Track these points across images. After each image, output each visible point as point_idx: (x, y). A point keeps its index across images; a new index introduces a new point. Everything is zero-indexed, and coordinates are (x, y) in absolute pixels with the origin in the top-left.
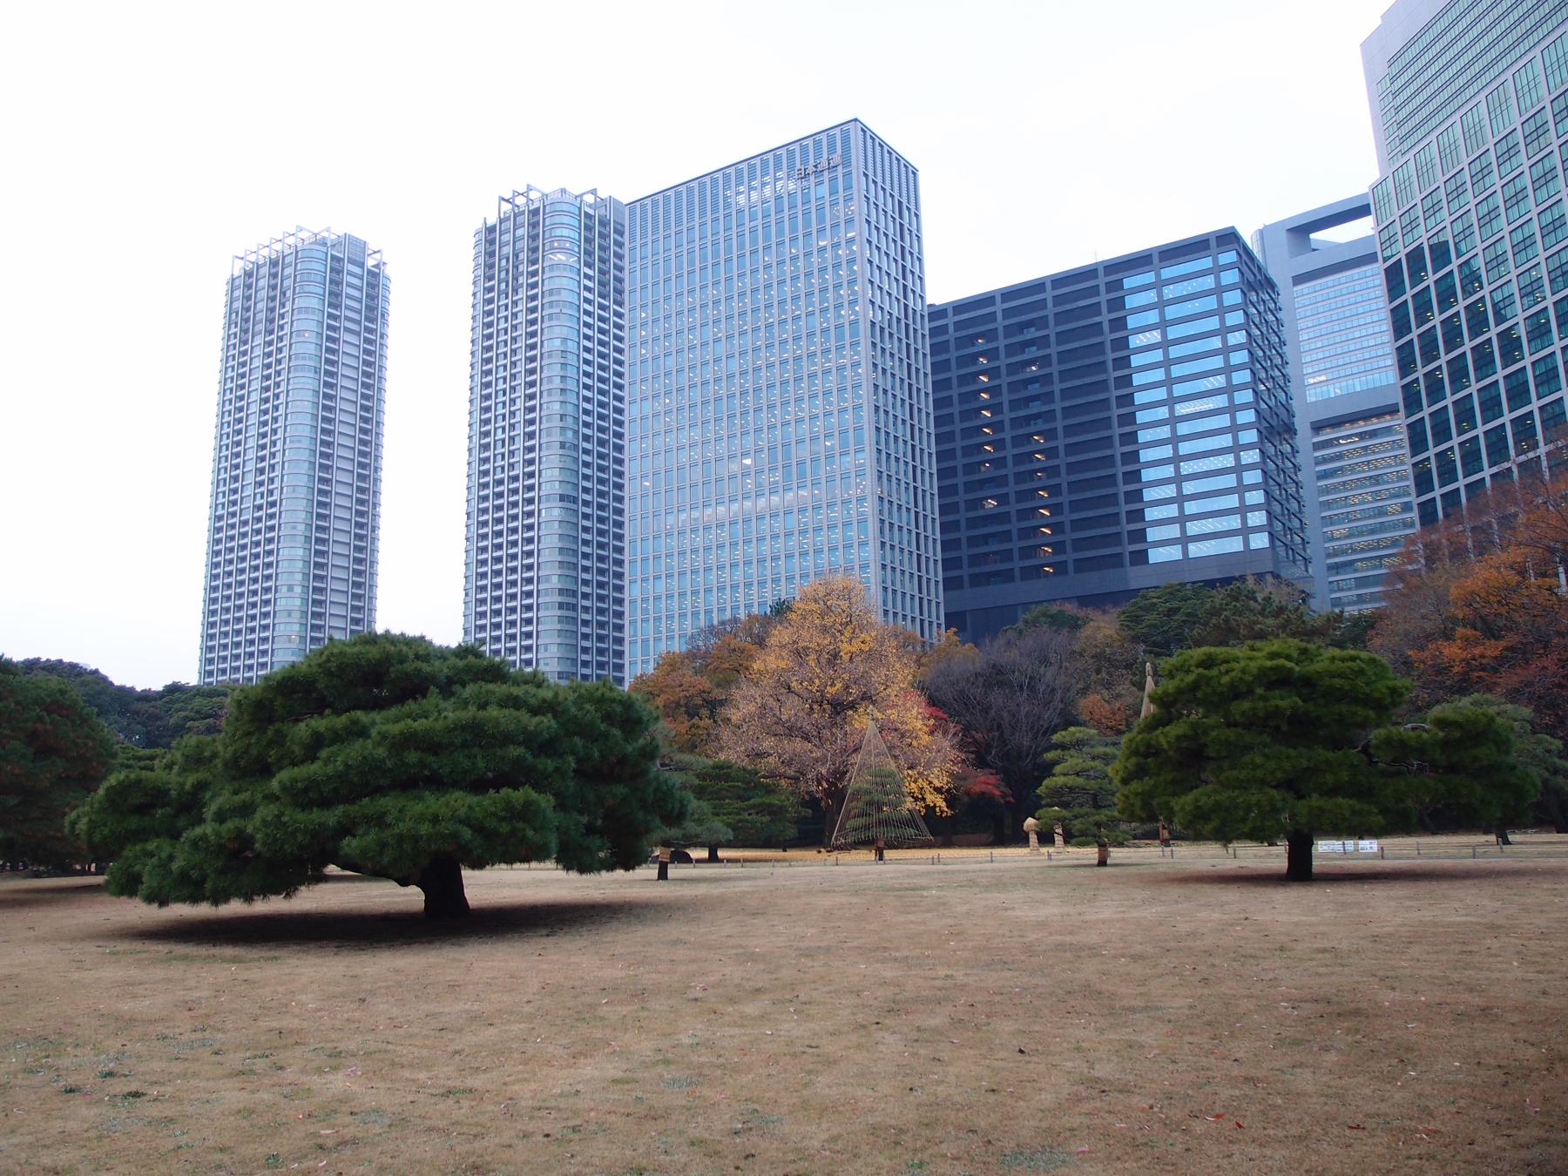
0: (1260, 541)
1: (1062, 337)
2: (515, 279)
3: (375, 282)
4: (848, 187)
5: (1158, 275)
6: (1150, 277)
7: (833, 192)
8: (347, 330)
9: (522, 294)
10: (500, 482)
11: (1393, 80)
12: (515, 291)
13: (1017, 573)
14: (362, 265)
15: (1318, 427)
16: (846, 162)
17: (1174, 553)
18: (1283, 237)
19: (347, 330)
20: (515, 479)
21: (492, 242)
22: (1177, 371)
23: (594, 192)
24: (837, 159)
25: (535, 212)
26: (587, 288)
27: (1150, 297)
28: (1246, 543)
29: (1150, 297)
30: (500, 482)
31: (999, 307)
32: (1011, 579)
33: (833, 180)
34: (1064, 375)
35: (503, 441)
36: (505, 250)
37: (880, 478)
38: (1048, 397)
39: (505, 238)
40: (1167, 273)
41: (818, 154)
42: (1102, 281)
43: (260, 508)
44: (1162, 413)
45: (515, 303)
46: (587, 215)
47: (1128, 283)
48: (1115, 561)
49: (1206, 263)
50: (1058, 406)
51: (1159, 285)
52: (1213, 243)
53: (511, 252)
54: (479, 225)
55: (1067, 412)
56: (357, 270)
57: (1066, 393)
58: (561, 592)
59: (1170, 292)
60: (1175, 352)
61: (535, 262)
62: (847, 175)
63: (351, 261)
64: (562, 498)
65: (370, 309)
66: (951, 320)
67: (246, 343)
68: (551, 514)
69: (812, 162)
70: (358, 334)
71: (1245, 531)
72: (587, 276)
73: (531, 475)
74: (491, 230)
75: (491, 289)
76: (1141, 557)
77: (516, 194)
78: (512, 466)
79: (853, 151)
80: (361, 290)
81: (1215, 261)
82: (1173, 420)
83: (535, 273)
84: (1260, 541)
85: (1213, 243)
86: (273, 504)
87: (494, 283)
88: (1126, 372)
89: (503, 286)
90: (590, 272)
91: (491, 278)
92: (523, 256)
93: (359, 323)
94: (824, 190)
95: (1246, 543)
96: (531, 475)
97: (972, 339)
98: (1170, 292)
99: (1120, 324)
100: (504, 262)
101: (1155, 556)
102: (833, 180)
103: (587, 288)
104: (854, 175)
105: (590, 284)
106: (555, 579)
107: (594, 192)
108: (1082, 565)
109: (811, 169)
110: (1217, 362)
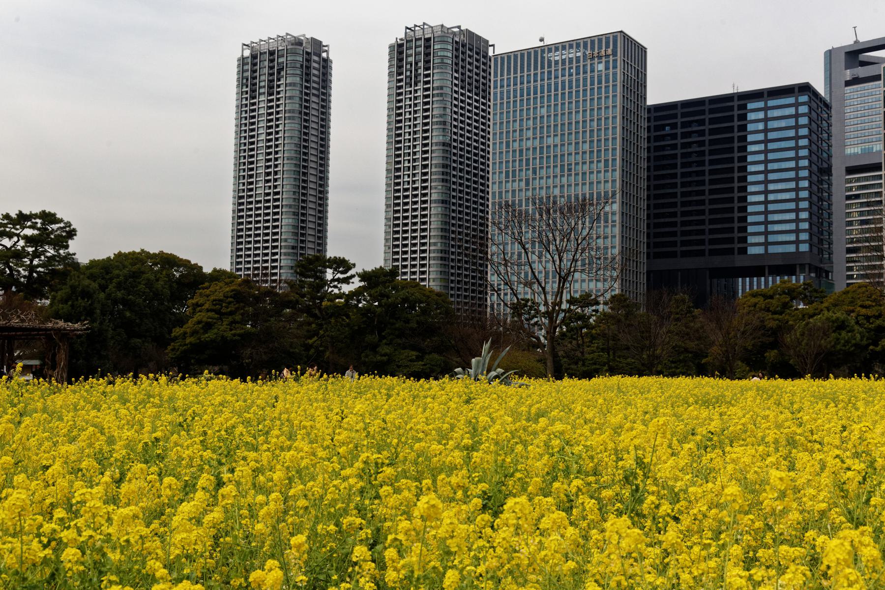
0: (804, 248)
1: (712, 132)
3: (326, 64)
5: (766, 104)
6: (761, 104)
8: (314, 95)
9: (420, 86)
10: (406, 190)
12: (416, 85)
13: (679, 253)
14: (319, 56)
15: (850, 170)
16: (614, 53)
17: (760, 250)
18: (843, 56)
19: (314, 95)
20: (416, 189)
21: (400, 53)
23: (459, 27)
24: (610, 51)
26: (456, 85)
28: (797, 248)
30: (406, 190)
31: (679, 111)
32: (676, 256)
33: (607, 62)
34: (712, 152)
35: (409, 167)
36: (410, 59)
39: (409, 52)
40: (771, 103)
42: (736, 103)
43: (268, 194)
45: (416, 91)
46: (456, 42)
47: (750, 106)
48: (731, 251)
49: (791, 100)
51: (766, 109)
52: (796, 90)
54: (393, 41)
55: (712, 172)
56: (316, 58)
57: (712, 162)
60: (771, 146)
61: (429, 69)
62: (615, 61)
63: (315, 54)
64: (443, 202)
65: (323, 81)
66: (653, 114)
67: (254, 98)
68: (435, 211)
70: (318, 96)
71: (797, 242)
72: (456, 78)
74: (400, 46)
76: (744, 251)
77: (416, 26)
83: (428, 76)
84: (804, 248)
85: (796, 90)
86: (278, 193)
87: (403, 77)
90: (457, 75)
92: (421, 64)
93: (318, 90)
94: (601, 67)
95: (797, 248)
97: (663, 127)
99: (743, 128)
100: (409, 66)
101: (752, 251)
102: (607, 62)
103: (456, 85)
105: (457, 82)
106: (439, 244)
107: (459, 27)
108: (713, 252)
110: (792, 154)
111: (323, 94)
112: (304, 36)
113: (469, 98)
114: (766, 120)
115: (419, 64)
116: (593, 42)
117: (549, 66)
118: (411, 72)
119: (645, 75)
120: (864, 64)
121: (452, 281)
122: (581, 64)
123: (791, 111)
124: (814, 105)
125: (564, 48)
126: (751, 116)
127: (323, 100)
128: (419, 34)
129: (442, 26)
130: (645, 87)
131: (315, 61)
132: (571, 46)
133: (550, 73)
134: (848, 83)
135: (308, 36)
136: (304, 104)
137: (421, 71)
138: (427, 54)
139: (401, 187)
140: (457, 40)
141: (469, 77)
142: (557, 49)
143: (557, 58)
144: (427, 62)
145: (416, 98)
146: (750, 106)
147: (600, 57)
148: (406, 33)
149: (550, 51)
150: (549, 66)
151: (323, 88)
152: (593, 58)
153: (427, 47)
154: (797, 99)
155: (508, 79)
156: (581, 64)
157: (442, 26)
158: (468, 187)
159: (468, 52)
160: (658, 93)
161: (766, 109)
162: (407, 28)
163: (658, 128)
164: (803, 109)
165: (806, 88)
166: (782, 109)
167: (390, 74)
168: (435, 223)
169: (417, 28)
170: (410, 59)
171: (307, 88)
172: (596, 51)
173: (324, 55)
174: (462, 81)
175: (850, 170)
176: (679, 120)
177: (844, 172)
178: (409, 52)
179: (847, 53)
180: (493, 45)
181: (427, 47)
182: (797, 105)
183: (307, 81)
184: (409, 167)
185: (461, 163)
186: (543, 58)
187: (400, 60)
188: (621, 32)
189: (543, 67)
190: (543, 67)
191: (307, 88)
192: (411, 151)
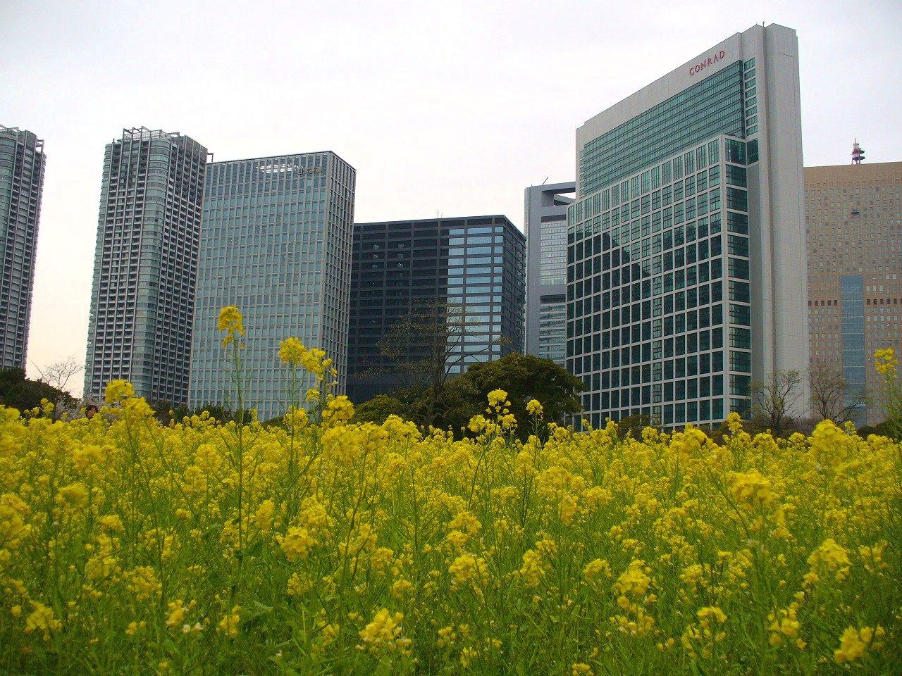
1: (417, 253)
2: (130, 179)
3: (39, 159)
4: (323, 185)
6: (461, 231)
7: (316, 185)
8: (24, 188)
9: (135, 188)
10: (114, 291)
11: (586, 155)
12: (130, 186)
14: (33, 150)
15: (545, 299)
16: (324, 172)
18: (540, 194)
19: (24, 188)
20: (123, 291)
22: (469, 281)
23: (178, 134)
25: (145, 143)
26: (170, 190)
27: (461, 241)
29: (461, 241)
33: (316, 179)
35: (117, 268)
37: (324, 328)
38: (406, 283)
39: (126, 154)
40: (471, 231)
41: (310, 165)
42: (439, 228)
44: (460, 300)
45: (129, 193)
47: (452, 232)
49: (488, 230)
50: (410, 288)
51: (466, 236)
52: (493, 221)
53: (129, 161)
56: (29, 152)
57: (415, 282)
58: (146, 356)
59: (471, 241)
60: (469, 271)
61: (143, 172)
62: (324, 179)
63: (28, 148)
65: (35, 175)
68: (143, 313)
69: (306, 167)
70: (28, 190)
72: (171, 183)
73: (132, 290)
74: (117, 147)
75: (114, 181)
77: (134, 129)
78: (121, 284)
79: (328, 168)
80: (31, 164)
81: (493, 230)
82: (464, 305)
83: (142, 178)
85: (493, 221)
88: (444, 286)
89: (122, 181)
90: (172, 180)
91: (115, 174)
92: (137, 167)
93: (29, 184)
94: (311, 183)
96: (132, 290)
98: (471, 241)
100: (124, 168)
103: (170, 190)
104: (327, 179)
105: (172, 187)
106: (143, 349)
107: (178, 134)
109: (306, 171)
111: (34, 188)
112: (17, 128)
113: (184, 203)
114: (466, 246)
115: (135, 167)
116: (303, 159)
117: (261, 178)
118: (126, 173)
119: (353, 194)
120: (558, 203)
121: (155, 387)
122: (292, 179)
123: (488, 240)
124: (509, 236)
125: (276, 162)
126: (452, 242)
127: (33, 195)
128: (136, 137)
129: (161, 131)
130: (353, 206)
131: (27, 155)
132: (283, 161)
133: (261, 184)
134: (545, 219)
135: (22, 129)
136: (12, 197)
137: (136, 173)
138: (144, 158)
139: (107, 288)
140: (175, 146)
141: (185, 183)
142: (269, 163)
143: (268, 172)
144: (143, 165)
145: (129, 199)
146: (452, 232)
147: (310, 174)
148: (124, 135)
149: (262, 163)
150: (261, 178)
151: (34, 182)
152: (302, 174)
153: (144, 150)
154: (493, 230)
155: (220, 188)
156: (292, 179)
157: (161, 131)
158: (176, 292)
159: (185, 158)
160: (365, 213)
161: (466, 236)
162: (125, 130)
163: (366, 246)
164: (499, 239)
165: (501, 220)
166: (480, 237)
167: (105, 174)
168: (141, 325)
169: (135, 131)
170: (125, 161)
171: (16, 181)
172: (306, 167)
173: (38, 150)
174: (177, 186)
175: (545, 299)
176: (387, 240)
177: (539, 300)
178: (126, 154)
179: (545, 192)
180: (212, 154)
181: (144, 150)
182: (493, 235)
183: (17, 174)
184: (117, 268)
185: (171, 267)
186: (255, 170)
187: (116, 161)
188: (331, 152)
189: (254, 179)
190: (254, 179)
191: (16, 181)
192: (120, 252)
